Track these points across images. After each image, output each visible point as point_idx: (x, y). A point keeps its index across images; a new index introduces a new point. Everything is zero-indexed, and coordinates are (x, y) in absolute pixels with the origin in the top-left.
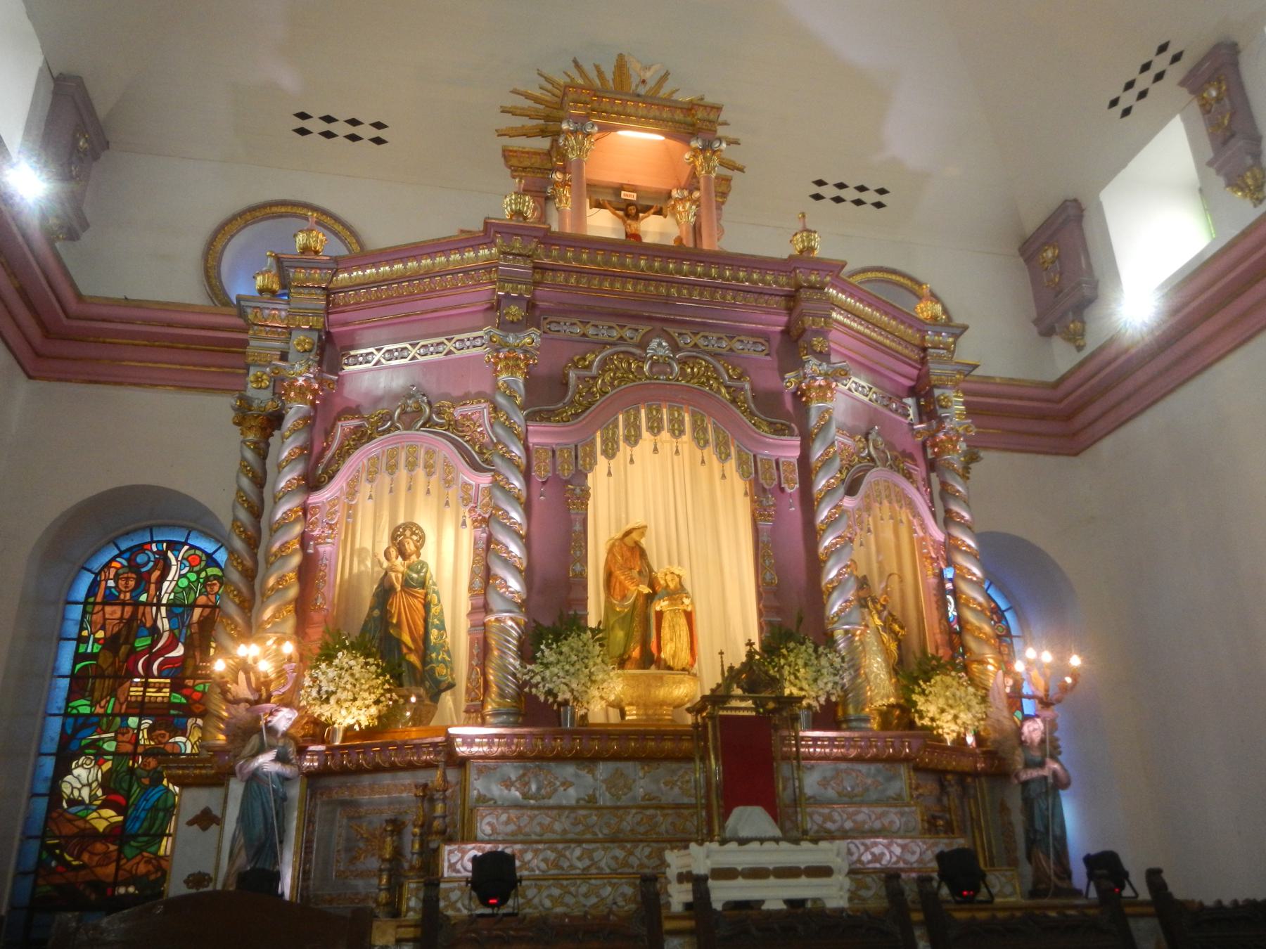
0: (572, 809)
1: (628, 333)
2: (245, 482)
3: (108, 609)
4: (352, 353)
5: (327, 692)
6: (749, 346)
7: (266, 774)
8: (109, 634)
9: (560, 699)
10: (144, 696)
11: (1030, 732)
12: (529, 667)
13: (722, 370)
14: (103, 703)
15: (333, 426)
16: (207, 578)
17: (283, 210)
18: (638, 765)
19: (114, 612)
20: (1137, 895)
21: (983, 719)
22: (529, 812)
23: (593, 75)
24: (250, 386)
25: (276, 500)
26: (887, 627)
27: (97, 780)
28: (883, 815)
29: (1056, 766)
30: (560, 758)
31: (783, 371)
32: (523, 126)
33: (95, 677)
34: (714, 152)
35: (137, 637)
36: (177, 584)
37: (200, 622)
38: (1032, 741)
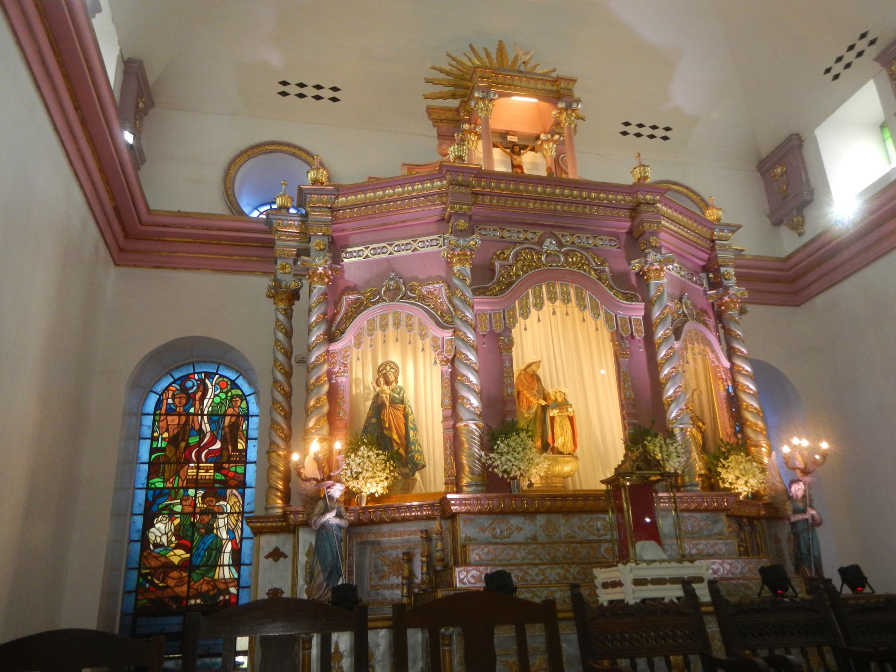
0: (526, 544)
1: (530, 236)
2: (280, 336)
3: (169, 418)
4: (349, 250)
5: (356, 472)
6: (606, 242)
7: (331, 526)
8: (171, 434)
9: (512, 475)
10: (197, 475)
11: (795, 491)
12: (491, 455)
13: (590, 259)
14: (171, 480)
15: (340, 299)
16: (232, 396)
17: (273, 147)
18: (561, 516)
19: (173, 420)
20: (874, 591)
21: (763, 483)
22: (501, 547)
23: (483, 54)
24: (278, 271)
27: (171, 530)
28: (715, 544)
29: (814, 512)
30: (514, 513)
31: (629, 260)
32: (440, 92)
33: (164, 463)
34: (573, 111)
35: (189, 436)
36: (213, 400)
37: (229, 426)
38: (797, 496)
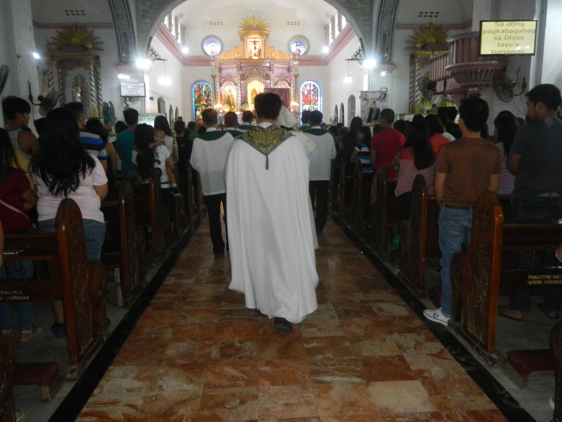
1: (251, 68)
2: (213, 84)
25: (217, 88)
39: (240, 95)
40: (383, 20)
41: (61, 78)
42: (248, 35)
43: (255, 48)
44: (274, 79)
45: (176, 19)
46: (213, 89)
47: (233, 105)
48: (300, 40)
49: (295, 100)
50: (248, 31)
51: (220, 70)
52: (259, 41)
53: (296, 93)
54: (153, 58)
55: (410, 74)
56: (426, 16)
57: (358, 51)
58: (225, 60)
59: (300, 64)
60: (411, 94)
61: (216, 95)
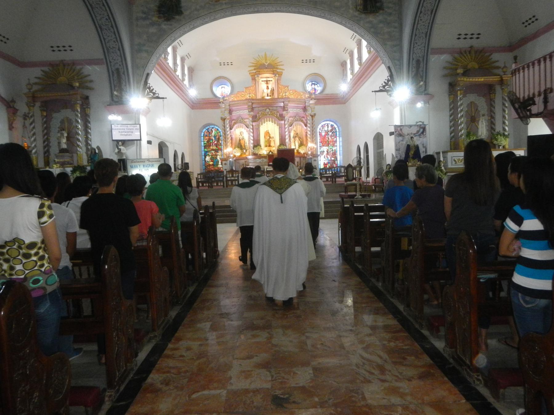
2: (223, 128)
25: (227, 132)
26: (299, 140)
30: (257, 158)
39: (252, 138)
40: (415, 43)
41: (45, 122)
42: (260, 74)
43: (268, 88)
44: (288, 120)
45: (183, 60)
46: (223, 132)
47: (245, 149)
48: (316, 78)
49: (312, 142)
50: (260, 70)
51: (230, 112)
52: (271, 81)
53: (313, 134)
54: (151, 96)
55: (450, 105)
56: (465, 38)
57: (386, 81)
58: (236, 101)
59: (316, 104)
60: (453, 128)
61: (226, 139)
